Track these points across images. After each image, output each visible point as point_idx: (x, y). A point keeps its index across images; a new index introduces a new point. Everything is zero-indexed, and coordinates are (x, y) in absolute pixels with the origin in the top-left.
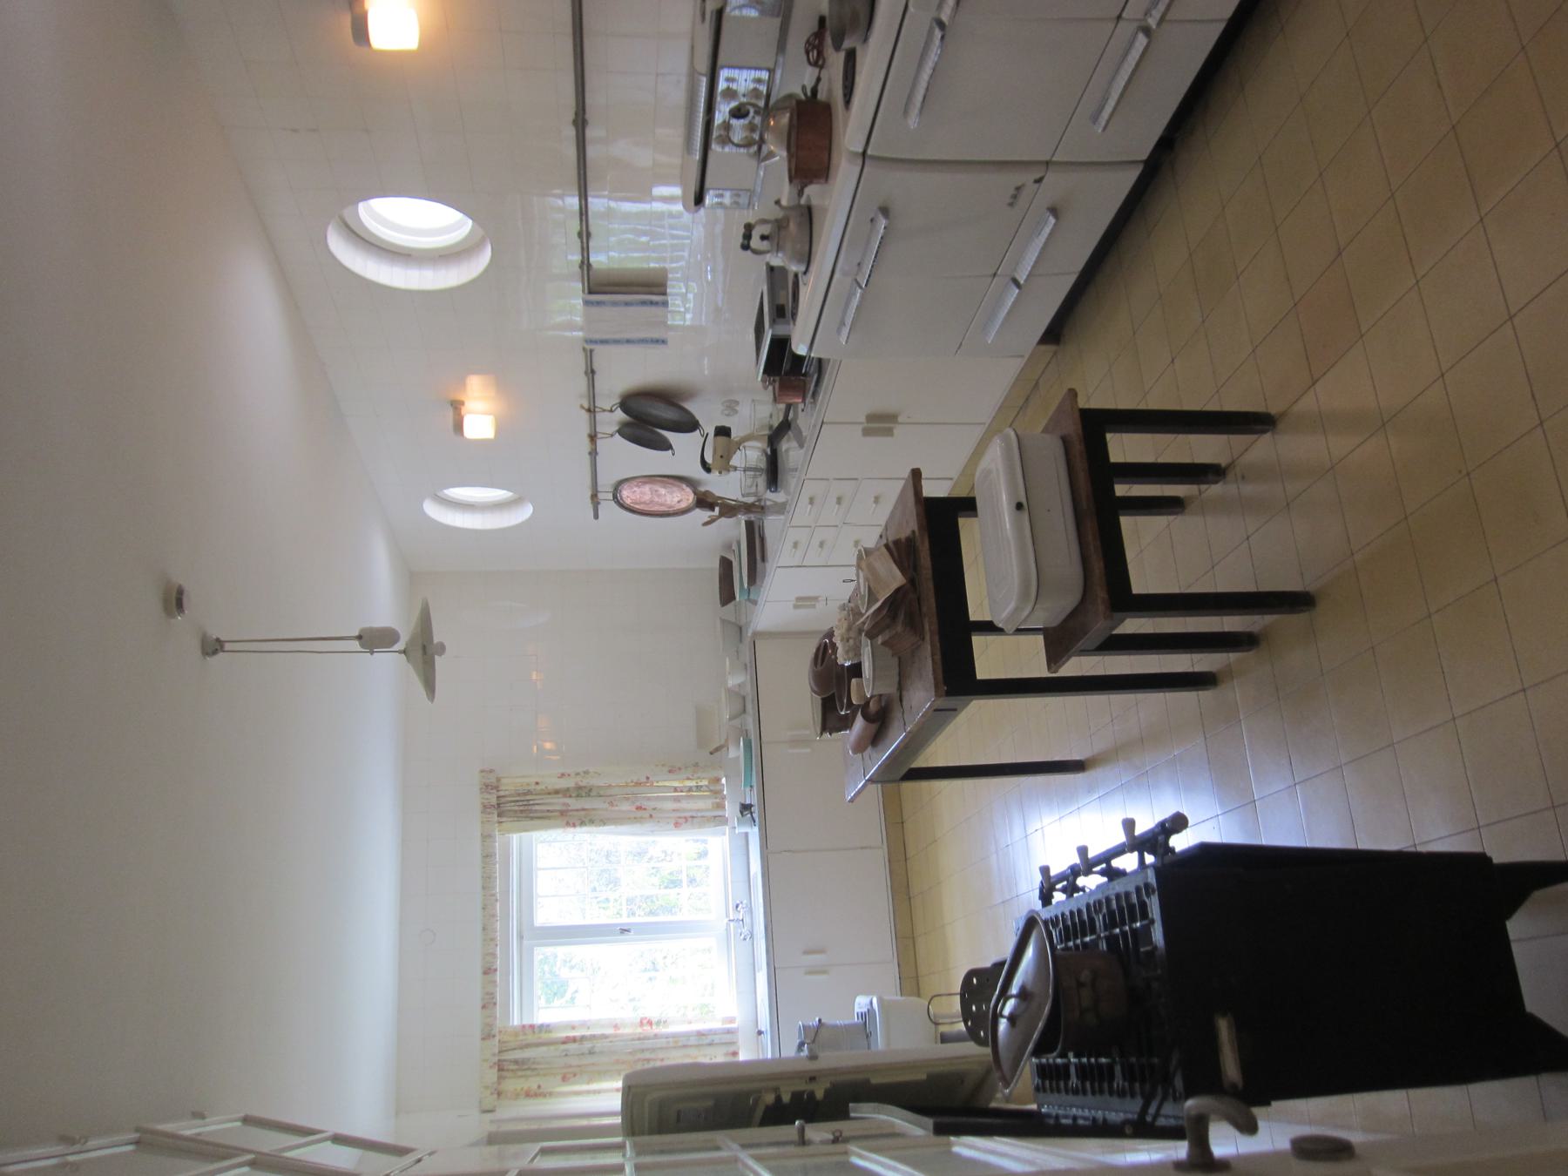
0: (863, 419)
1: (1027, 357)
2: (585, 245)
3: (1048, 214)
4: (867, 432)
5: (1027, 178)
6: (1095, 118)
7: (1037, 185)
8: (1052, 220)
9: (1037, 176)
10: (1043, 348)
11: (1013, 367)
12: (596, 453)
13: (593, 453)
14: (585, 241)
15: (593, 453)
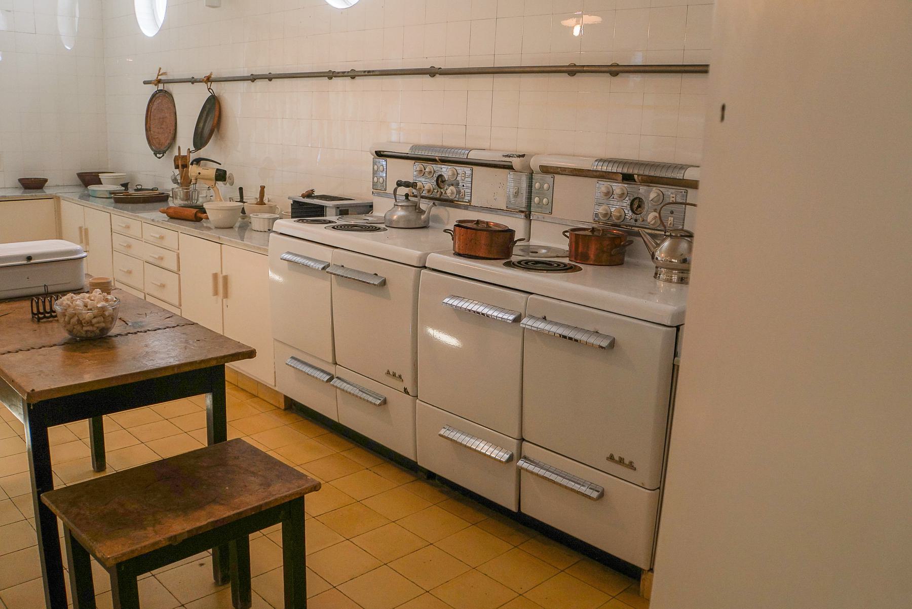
0: (224, 274)
1: (276, 389)
2: (346, 74)
3: (382, 399)
4: (215, 276)
5: (408, 383)
6: (451, 427)
7: (403, 390)
8: (378, 402)
9: (409, 390)
10: (282, 400)
11: (270, 382)
12: (193, 83)
13: (193, 81)
14: (349, 74)
15: (193, 81)
